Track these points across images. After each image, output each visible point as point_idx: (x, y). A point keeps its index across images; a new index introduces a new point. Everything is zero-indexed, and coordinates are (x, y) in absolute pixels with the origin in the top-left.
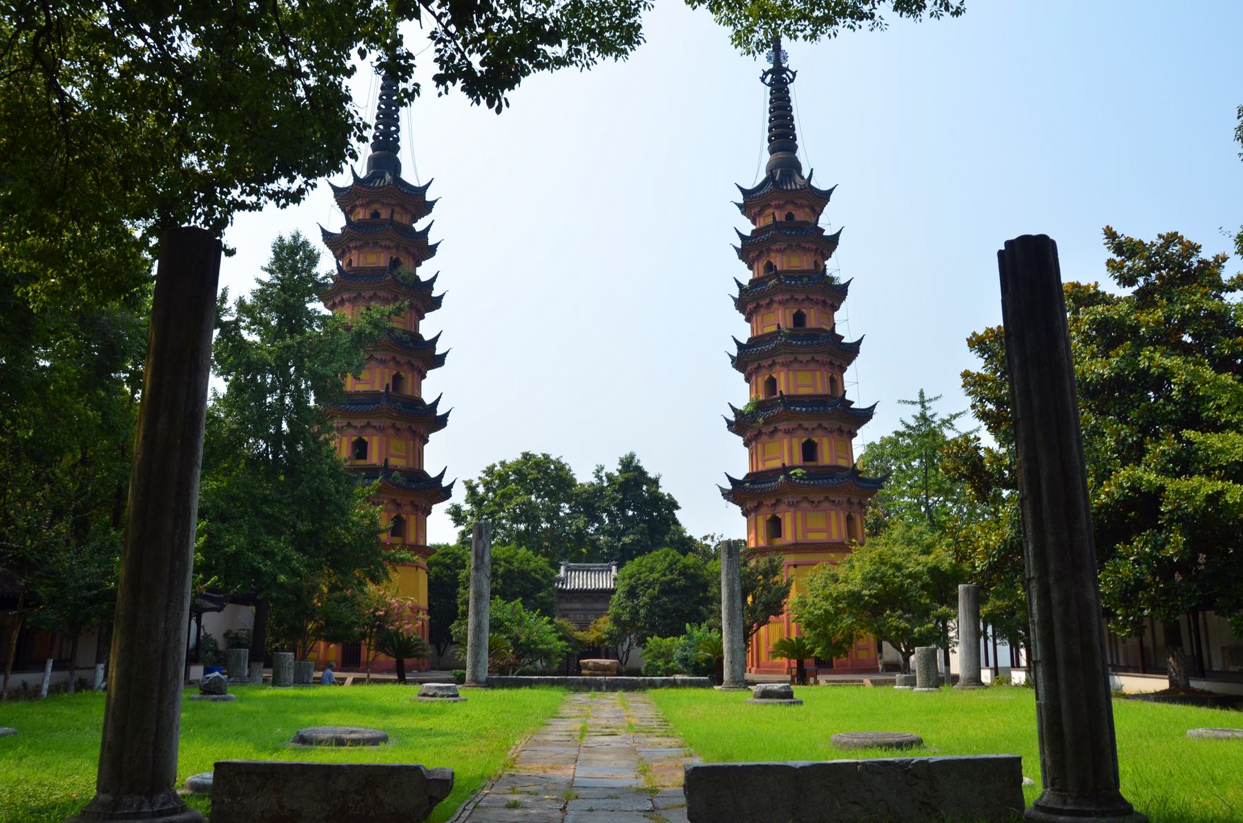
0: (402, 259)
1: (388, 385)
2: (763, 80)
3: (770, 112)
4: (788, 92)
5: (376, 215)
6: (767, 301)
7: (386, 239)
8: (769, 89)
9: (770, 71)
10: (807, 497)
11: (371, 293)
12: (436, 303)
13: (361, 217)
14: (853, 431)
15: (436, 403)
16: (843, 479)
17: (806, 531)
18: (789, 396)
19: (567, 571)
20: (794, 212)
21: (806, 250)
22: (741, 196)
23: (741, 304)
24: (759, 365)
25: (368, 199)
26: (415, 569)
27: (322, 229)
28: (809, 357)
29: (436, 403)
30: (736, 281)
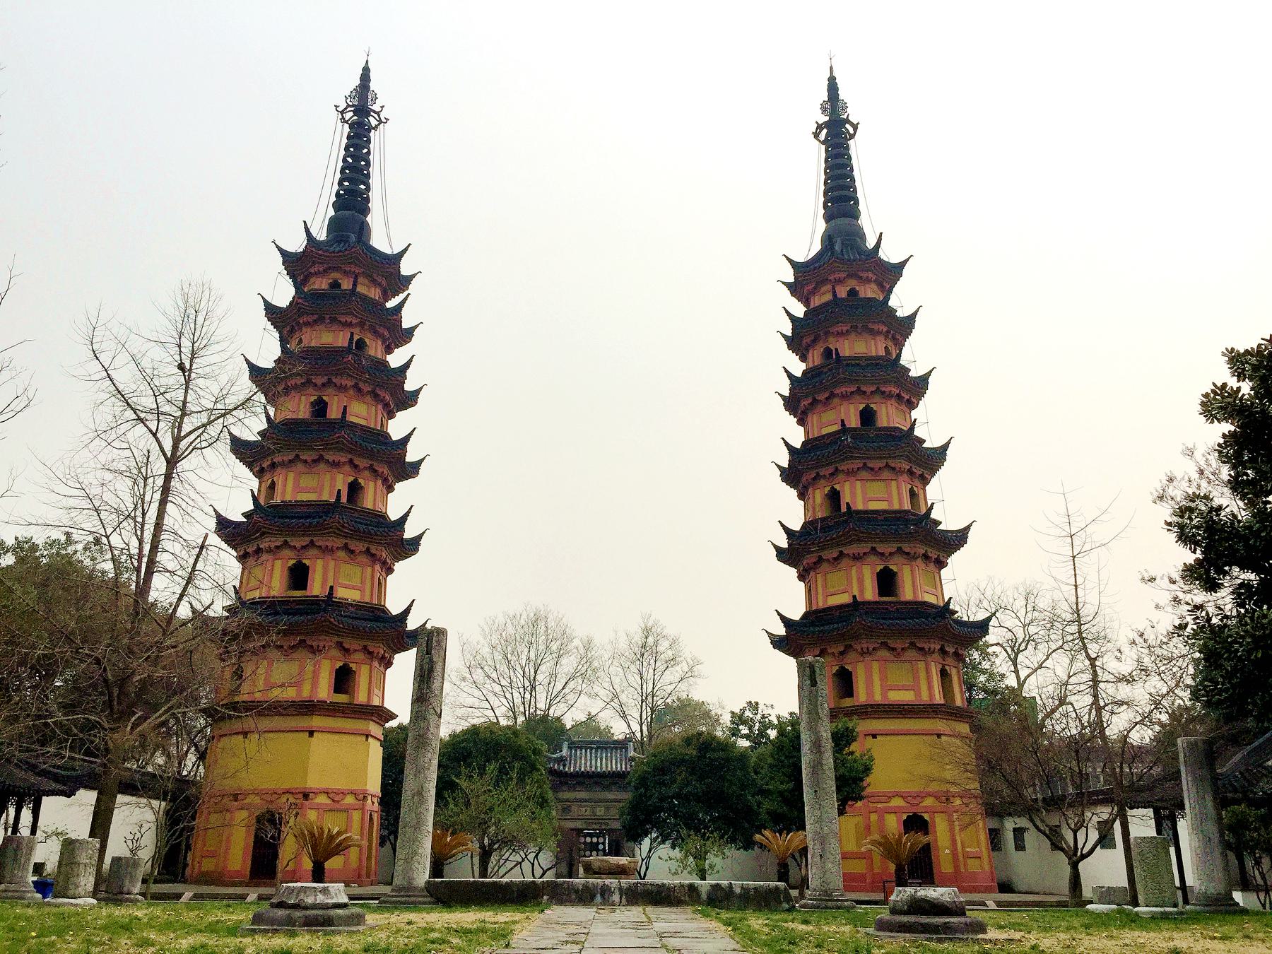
0: (366, 340)
1: (339, 491)
2: (816, 135)
4: (848, 148)
5: (335, 285)
6: (826, 395)
9: (826, 124)
11: (324, 380)
15: (404, 518)
18: (858, 512)
19: (570, 748)
20: (857, 288)
21: (874, 333)
22: (791, 271)
24: (818, 473)
25: (325, 266)
26: (364, 738)
27: (265, 301)
29: (404, 518)
30: (786, 371)
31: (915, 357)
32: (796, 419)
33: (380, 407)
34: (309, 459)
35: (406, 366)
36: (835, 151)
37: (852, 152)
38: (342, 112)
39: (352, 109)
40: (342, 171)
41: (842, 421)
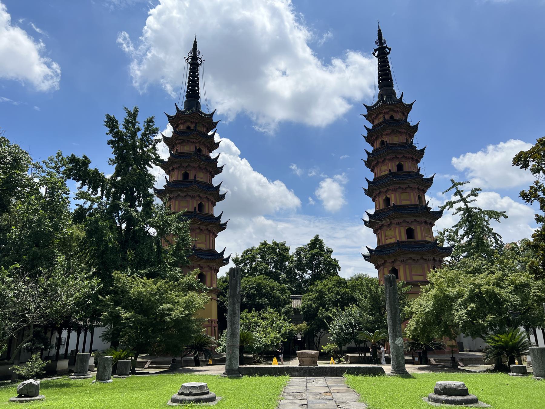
0: (202, 148)
1: (195, 207)
2: (374, 54)
3: (378, 69)
5: (189, 127)
6: (383, 159)
7: (194, 138)
8: (377, 58)
9: (378, 49)
11: (187, 164)
12: (219, 170)
13: (181, 129)
14: (432, 222)
15: (220, 216)
16: (430, 247)
17: (412, 275)
18: (397, 206)
20: (394, 115)
21: (401, 133)
23: (368, 164)
24: (380, 191)
25: (184, 120)
28: (406, 186)
29: (220, 216)
31: (418, 142)
32: (370, 170)
33: (208, 174)
35: (217, 157)
36: (382, 60)
38: (187, 59)
40: (188, 83)
41: (390, 170)
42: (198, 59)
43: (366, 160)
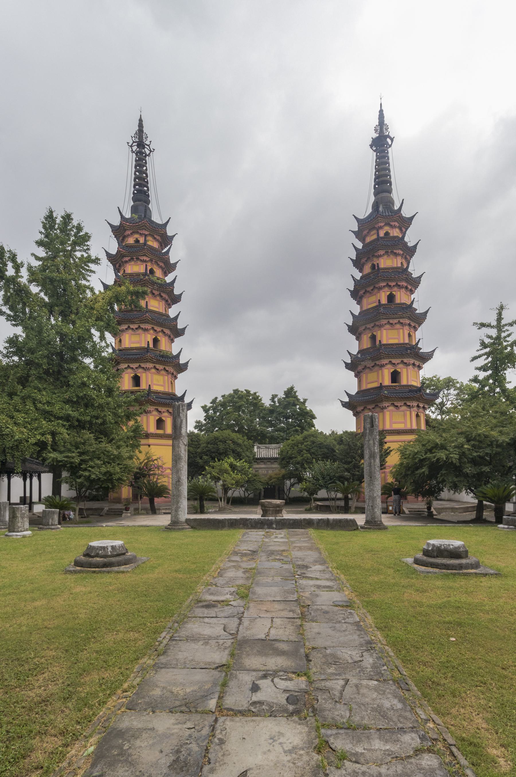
0: (155, 269)
3: (376, 168)
5: (137, 241)
8: (375, 153)
10: (393, 404)
14: (421, 365)
20: (389, 231)
21: (396, 255)
34: (134, 328)
37: (390, 155)
38: (131, 146)
39: (136, 144)
42: (146, 146)
43: (352, 289)
